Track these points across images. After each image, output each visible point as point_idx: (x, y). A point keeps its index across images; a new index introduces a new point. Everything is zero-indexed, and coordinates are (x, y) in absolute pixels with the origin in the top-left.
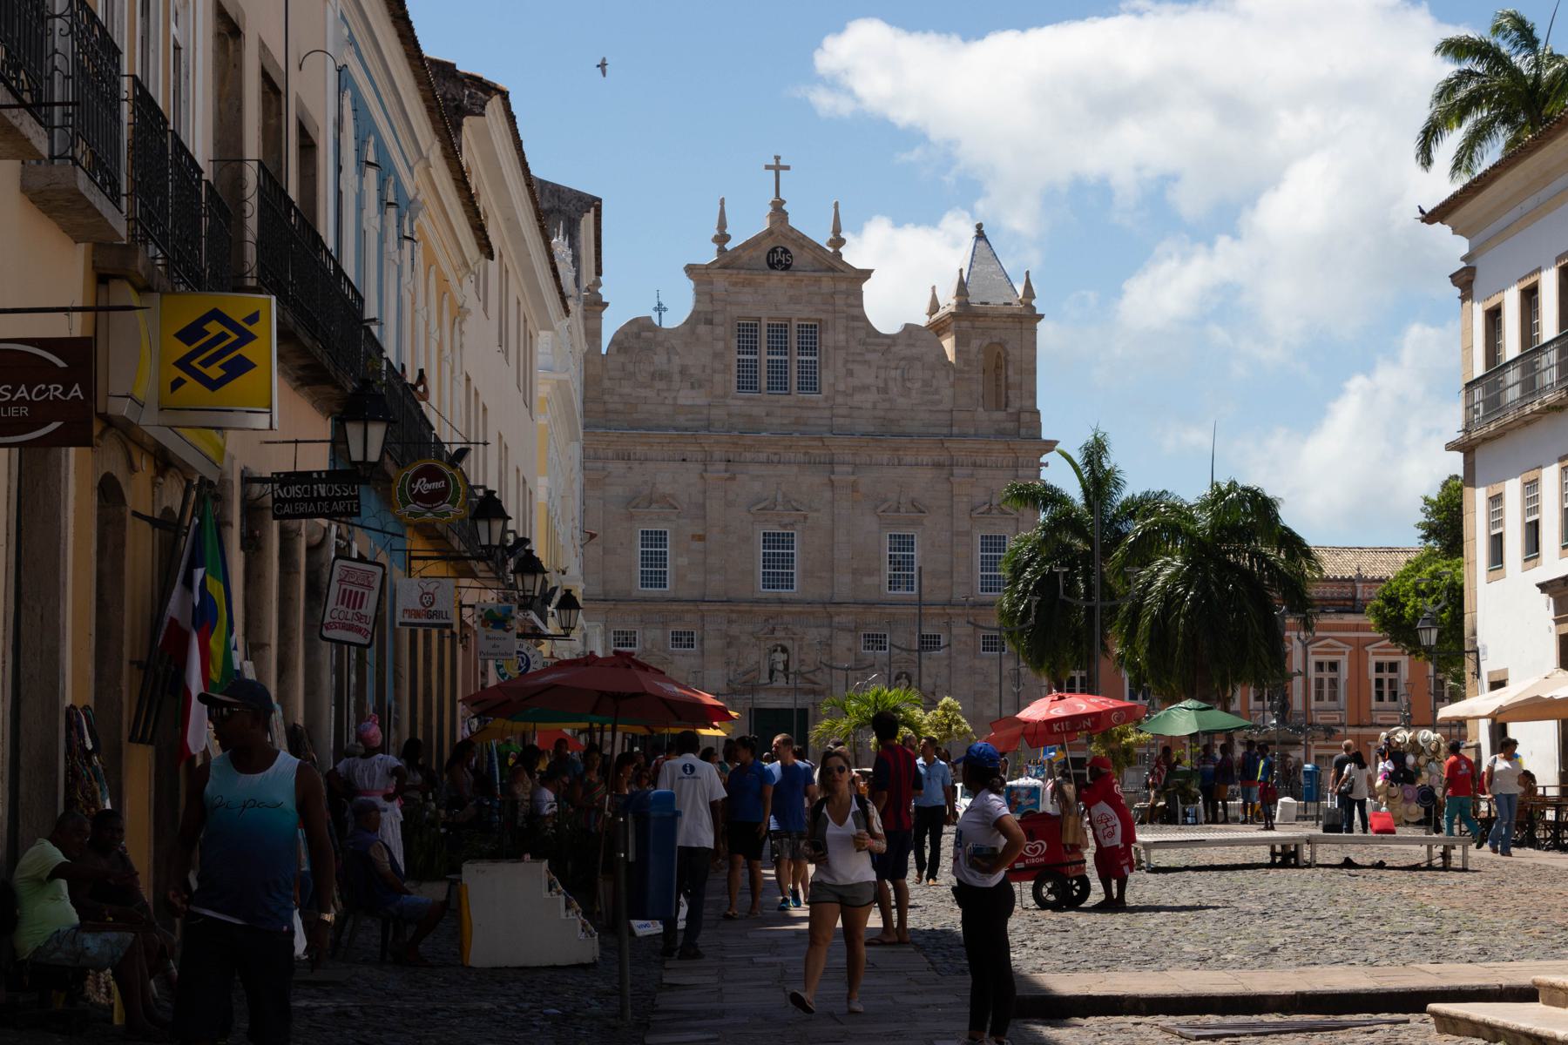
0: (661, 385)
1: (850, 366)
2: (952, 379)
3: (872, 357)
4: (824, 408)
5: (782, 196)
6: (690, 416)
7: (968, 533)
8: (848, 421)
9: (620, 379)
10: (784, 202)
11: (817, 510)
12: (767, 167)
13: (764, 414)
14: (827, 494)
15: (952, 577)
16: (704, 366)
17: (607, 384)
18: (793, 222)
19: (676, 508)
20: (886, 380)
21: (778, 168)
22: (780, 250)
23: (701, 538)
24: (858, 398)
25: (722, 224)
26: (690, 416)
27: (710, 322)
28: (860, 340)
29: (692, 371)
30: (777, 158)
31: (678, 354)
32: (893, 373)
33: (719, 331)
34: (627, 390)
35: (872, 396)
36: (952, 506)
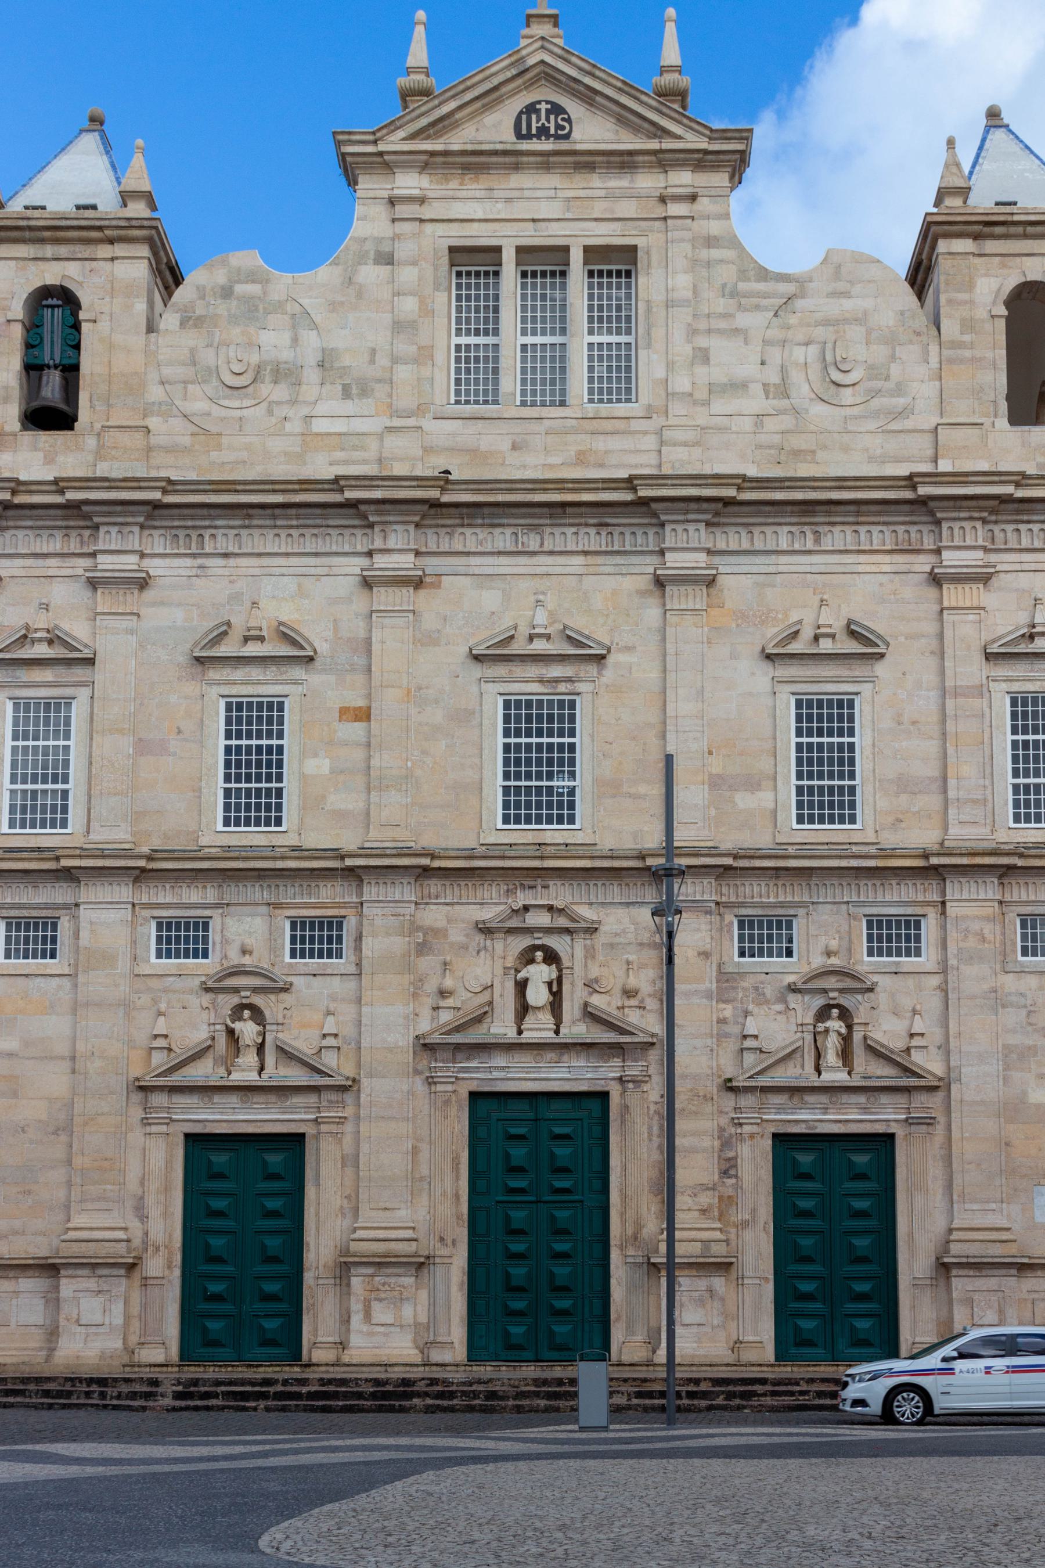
0: (280, 392)
1: (702, 342)
2: (934, 361)
3: (752, 321)
4: (645, 433)
6: (339, 455)
7: (980, 691)
8: (697, 452)
9: (185, 382)
11: (629, 649)
13: (505, 445)
14: (652, 613)
15: (945, 790)
16: (373, 352)
17: (155, 393)
19: (302, 648)
20: (783, 369)
22: (543, 107)
23: (364, 715)
24: (719, 406)
26: (339, 455)
27: (387, 259)
28: (724, 286)
29: (347, 361)
31: (314, 326)
32: (799, 354)
33: (407, 275)
34: (199, 406)
35: (755, 402)
36: (941, 636)
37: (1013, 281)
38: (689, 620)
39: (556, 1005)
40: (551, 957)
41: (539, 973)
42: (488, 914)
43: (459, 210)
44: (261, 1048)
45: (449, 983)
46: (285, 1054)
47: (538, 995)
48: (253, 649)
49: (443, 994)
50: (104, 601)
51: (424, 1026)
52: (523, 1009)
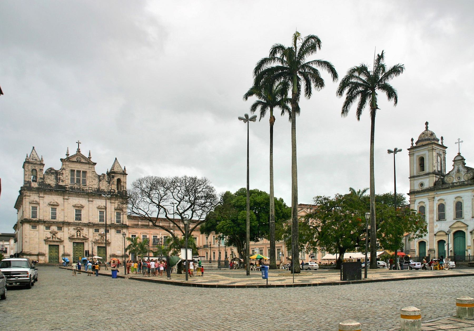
5: (79, 148)
10: (80, 149)
12: (77, 143)
18: (81, 153)
21: (79, 143)
25: (68, 152)
30: (79, 141)
37: (117, 178)
38: (91, 204)
39: (80, 235)
40: (80, 231)
41: (79, 233)
42: (75, 228)
43: (72, 166)
44: (55, 238)
45: (71, 233)
46: (58, 238)
47: (79, 234)
48: (54, 204)
49: (71, 234)
50: (41, 198)
51: (69, 236)
52: (77, 235)
